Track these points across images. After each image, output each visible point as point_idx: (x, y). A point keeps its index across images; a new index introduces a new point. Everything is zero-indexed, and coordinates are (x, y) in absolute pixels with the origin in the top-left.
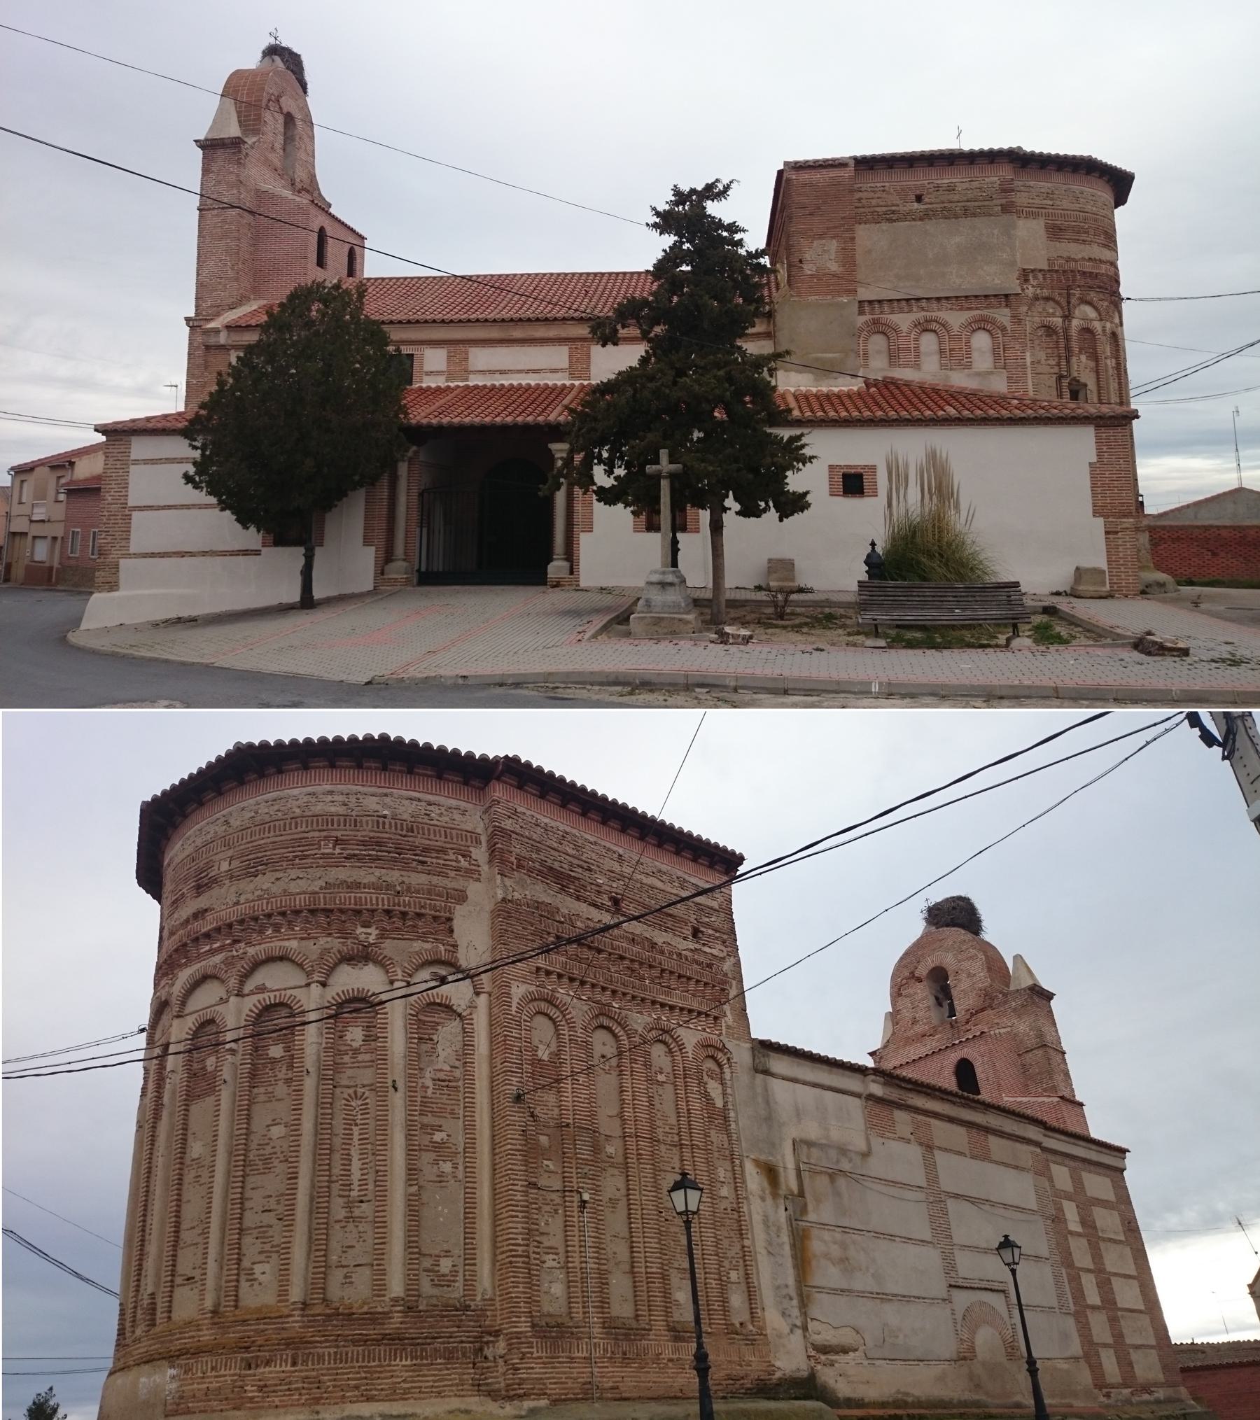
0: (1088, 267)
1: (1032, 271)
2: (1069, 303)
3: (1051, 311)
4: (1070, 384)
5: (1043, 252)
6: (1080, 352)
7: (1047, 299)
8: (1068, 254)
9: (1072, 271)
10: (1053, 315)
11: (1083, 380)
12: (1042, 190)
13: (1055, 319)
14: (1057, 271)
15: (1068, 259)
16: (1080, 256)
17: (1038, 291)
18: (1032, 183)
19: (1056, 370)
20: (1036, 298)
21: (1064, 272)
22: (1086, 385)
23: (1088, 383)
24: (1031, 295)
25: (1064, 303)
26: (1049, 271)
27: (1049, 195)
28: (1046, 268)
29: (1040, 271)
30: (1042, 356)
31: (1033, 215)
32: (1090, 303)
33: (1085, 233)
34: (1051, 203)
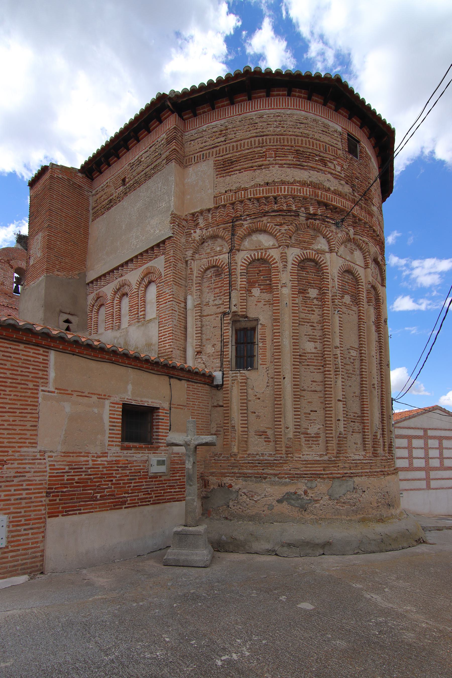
0: (261, 193)
1: (201, 212)
2: (233, 235)
3: (218, 249)
4: (234, 322)
5: (210, 191)
6: (251, 284)
7: (214, 237)
8: (237, 185)
9: (241, 202)
10: (221, 253)
11: (252, 314)
12: (214, 130)
13: (221, 257)
14: (224, 206)
15: (239, 189)
16: (253, 183)
17: (204, 231)
18: (204, 128)
19: (222, 310)
20: (203, 241)
21: (233, 204)
22: (257, 320)
23: (261, 318)
24: (197, 238)
25: (228, 236)
26: (217, 208)
27: (223, 132)
28: (212, 206)
29: (209, 210)
30: (209, 297)
31: (205, 158)
32: (264, 231)
33: (262, 157)
34: (223, 139)
